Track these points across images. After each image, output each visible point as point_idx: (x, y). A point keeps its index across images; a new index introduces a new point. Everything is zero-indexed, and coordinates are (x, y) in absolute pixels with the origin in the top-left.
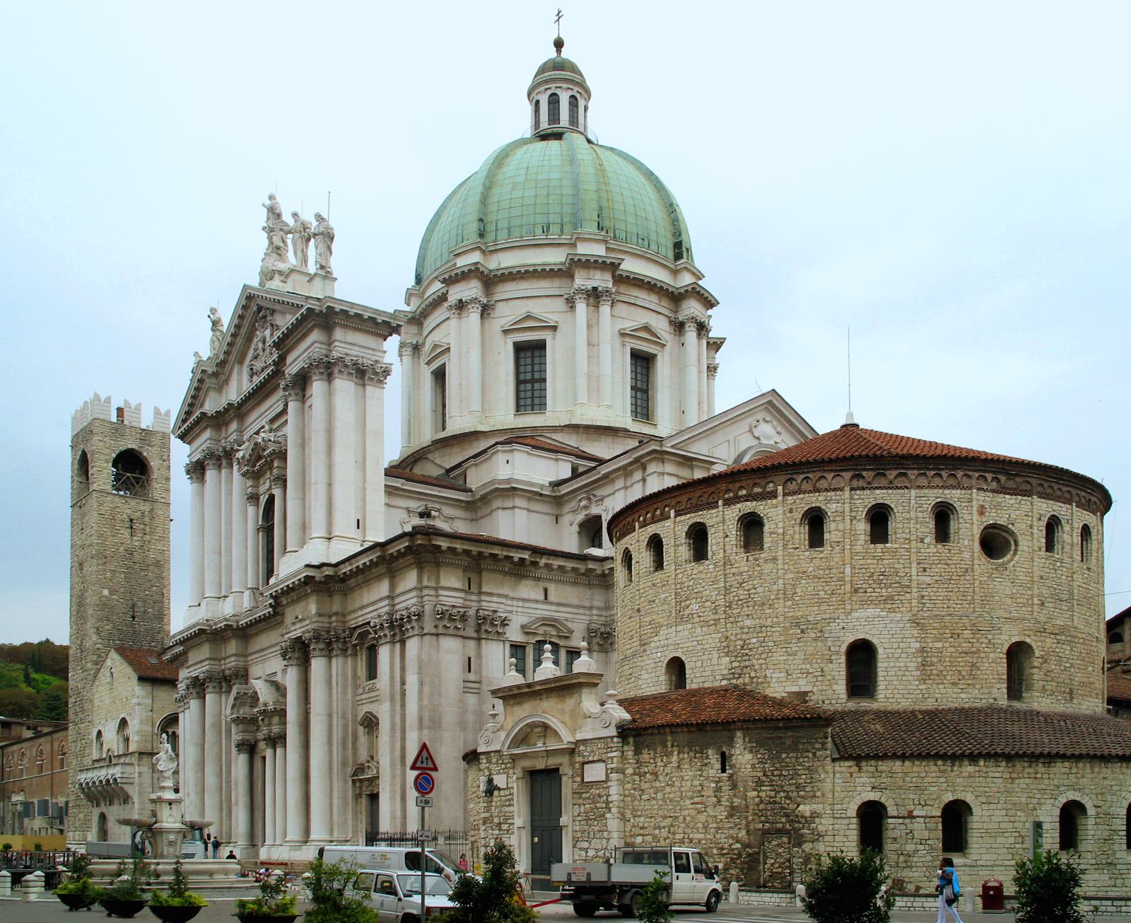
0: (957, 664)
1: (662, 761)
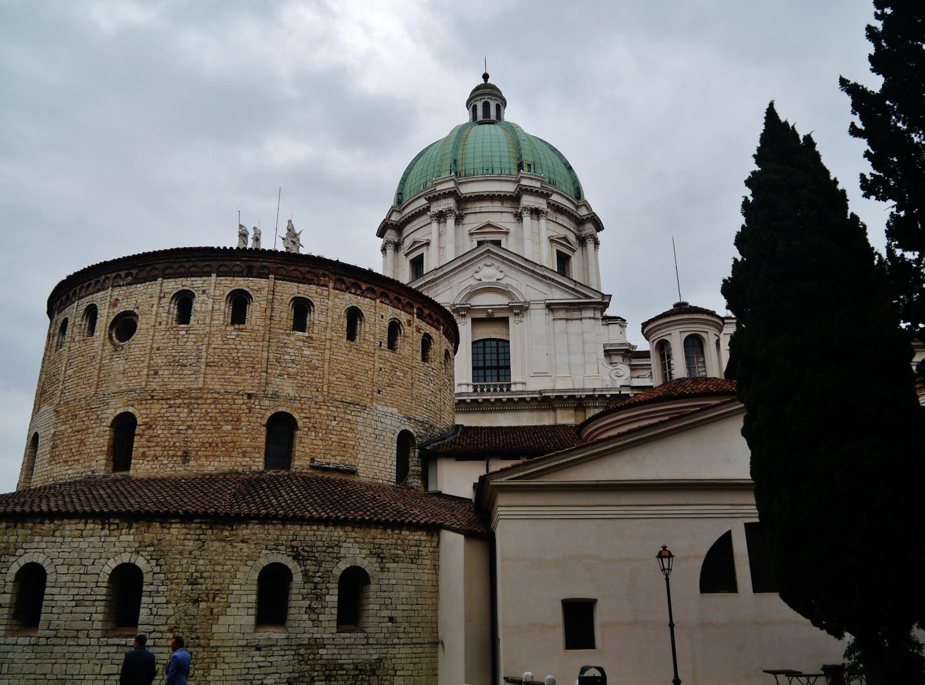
0: (70, 442)
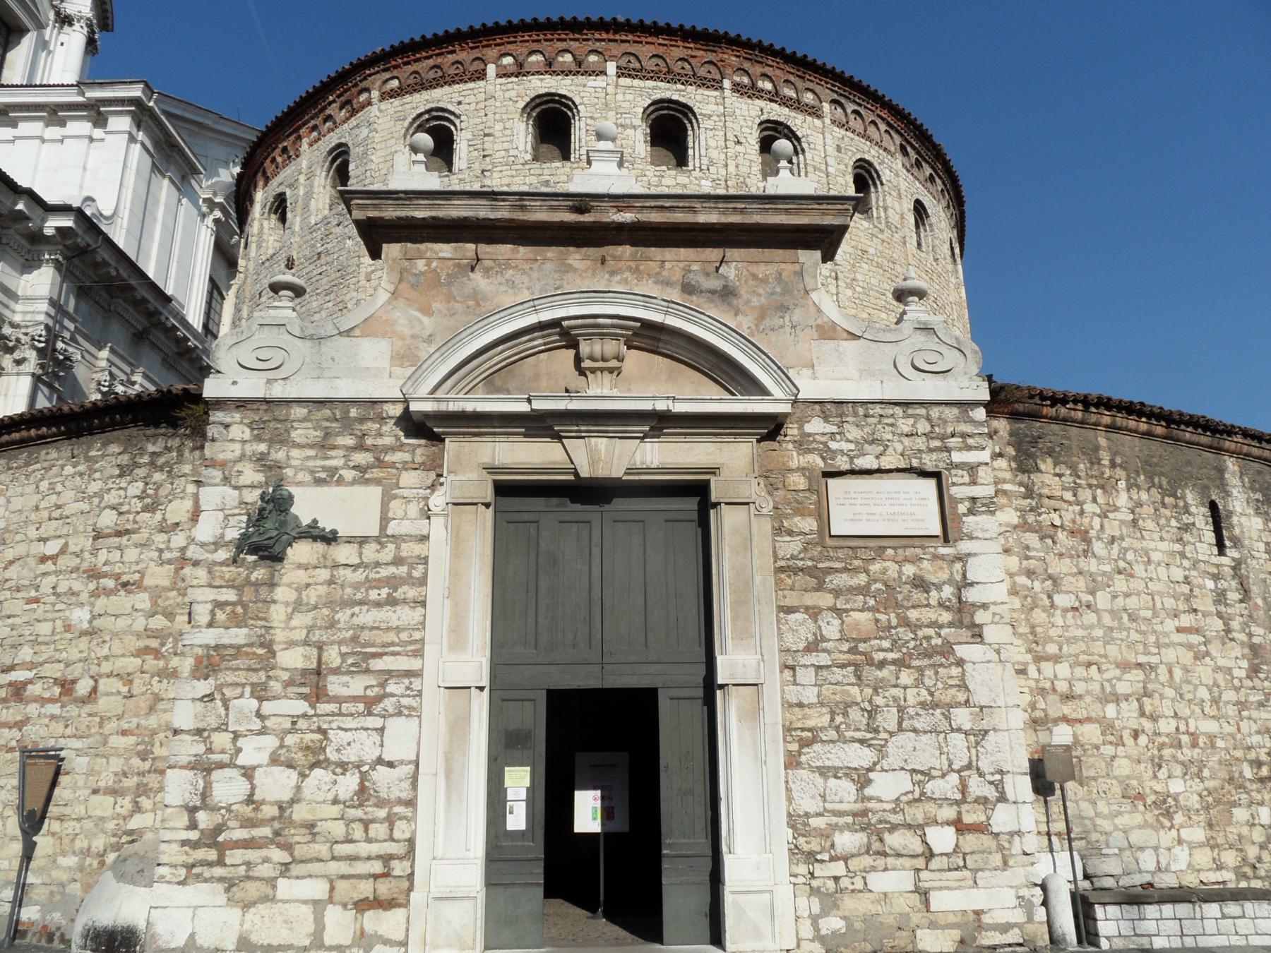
1: (1094, 500)
